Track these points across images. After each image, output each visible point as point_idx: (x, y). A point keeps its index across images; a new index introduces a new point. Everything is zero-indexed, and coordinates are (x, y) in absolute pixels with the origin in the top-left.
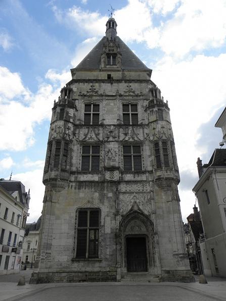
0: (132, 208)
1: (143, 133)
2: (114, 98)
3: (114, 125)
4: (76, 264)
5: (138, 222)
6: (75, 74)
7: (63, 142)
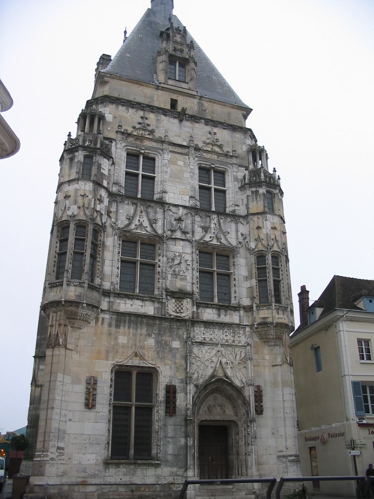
0: (213, 373)
1: (237, 231)
2: (186, 151)
3: (184, 207)
4: (112, 470)
5: (220, 399)
6: (106, 83)
7: (90, 228)
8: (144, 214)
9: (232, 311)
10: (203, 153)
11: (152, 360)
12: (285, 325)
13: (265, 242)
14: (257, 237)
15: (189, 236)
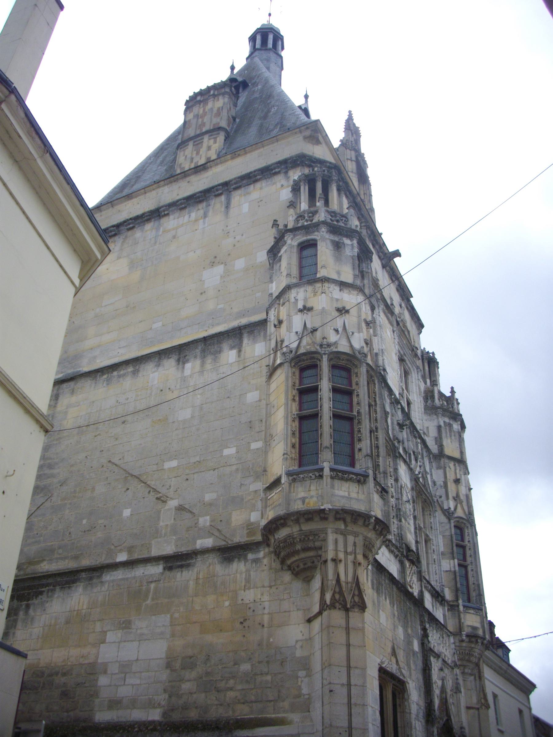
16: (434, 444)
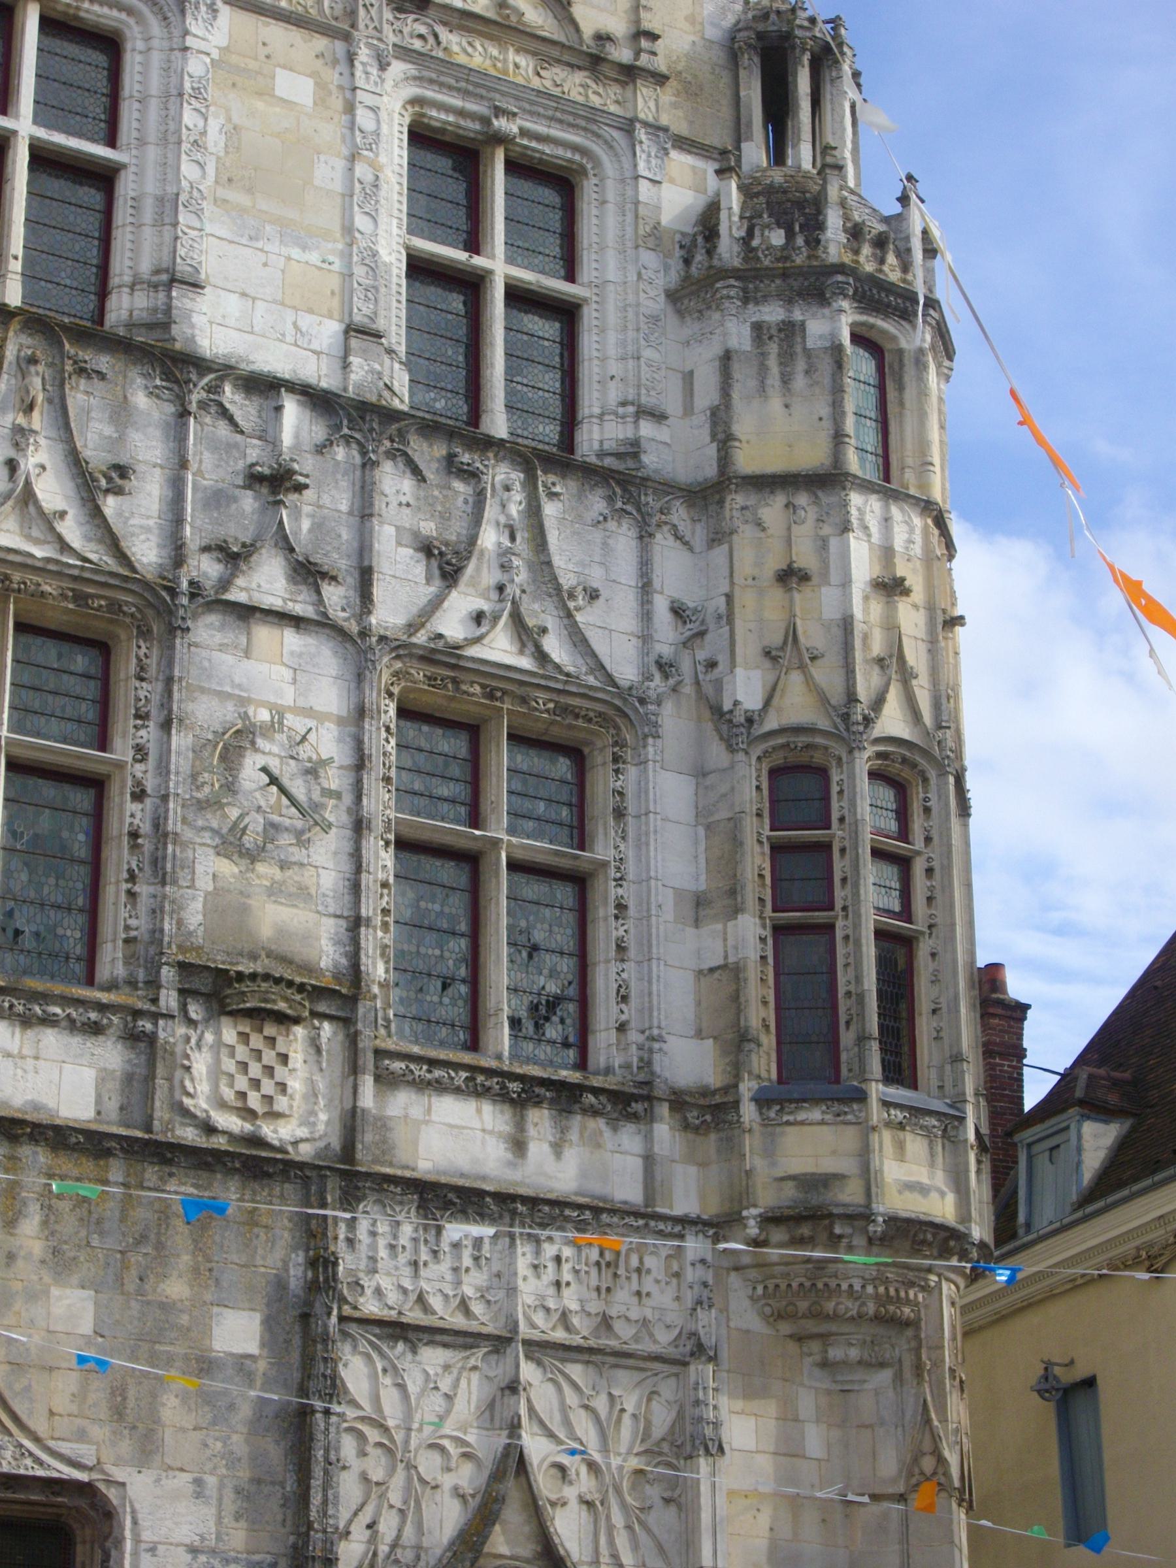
1: (646, 588)
8: (37, 420)
9: (601, 1123)
10: (444, 34)
11: (81, 1436)
12: (943, 1234)
13: (827, 675)
14: (776, 639)
15: (336, 597)
16: (708, 439)
